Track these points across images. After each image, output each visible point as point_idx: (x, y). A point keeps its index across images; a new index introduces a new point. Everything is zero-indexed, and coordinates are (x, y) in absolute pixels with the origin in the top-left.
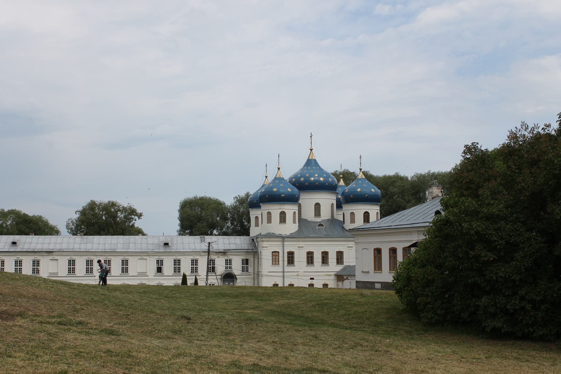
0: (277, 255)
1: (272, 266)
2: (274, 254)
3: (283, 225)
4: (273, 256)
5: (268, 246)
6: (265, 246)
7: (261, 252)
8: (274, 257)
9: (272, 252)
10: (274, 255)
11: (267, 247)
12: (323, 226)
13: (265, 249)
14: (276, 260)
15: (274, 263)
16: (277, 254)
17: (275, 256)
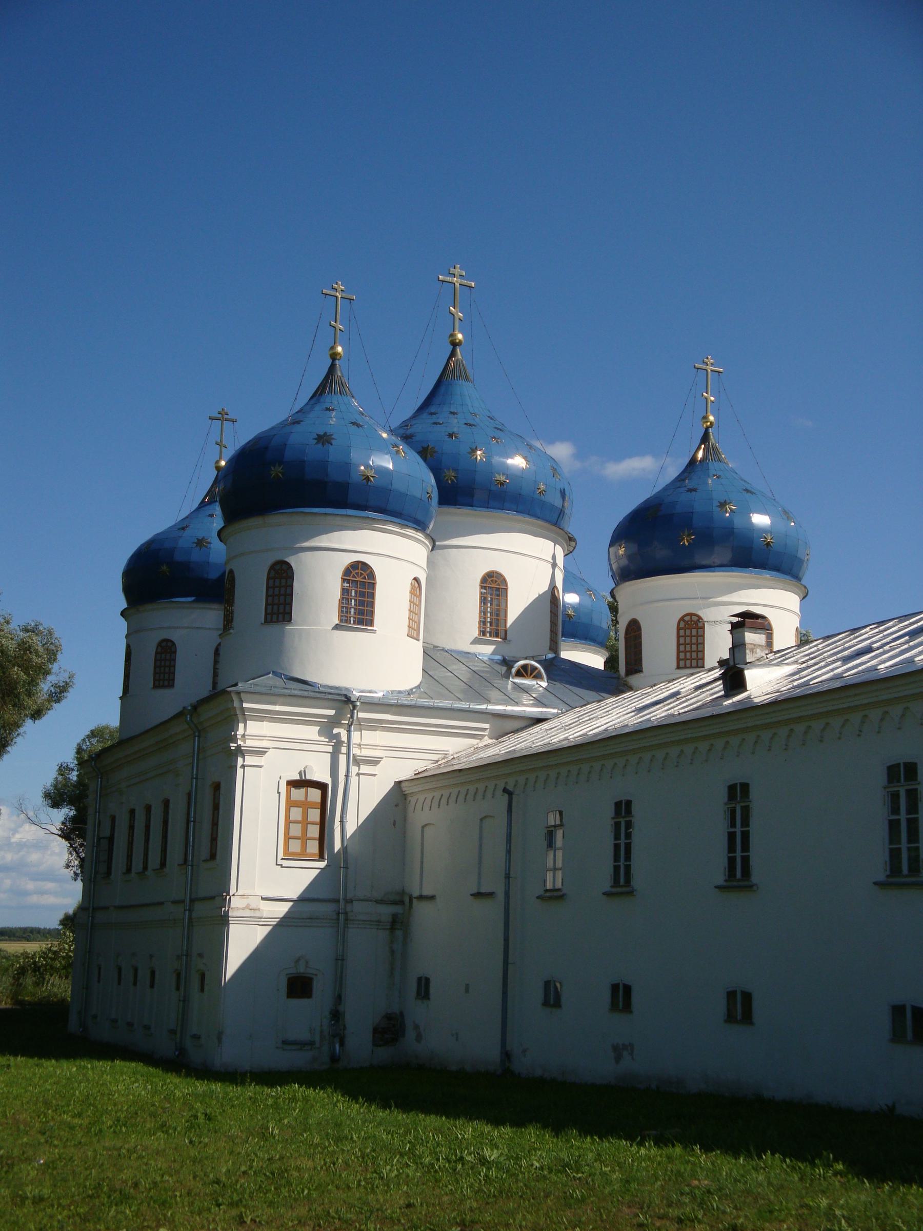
0: (312, 805)
1: (285, 863)
2: (298, 794)
3: (354, 639)
4: (290, 804)
5: (264, 744)
6: (249, 743)
7: (217, 787)
8: (296, 813)
9: (292, 784)
10: (296, 804)
11: (260, 752)
12: (538, 677)
13: (249, 760)
14: (305, 831)
15: (295, 846)
16: (315, 795)
17: (305, 805)
